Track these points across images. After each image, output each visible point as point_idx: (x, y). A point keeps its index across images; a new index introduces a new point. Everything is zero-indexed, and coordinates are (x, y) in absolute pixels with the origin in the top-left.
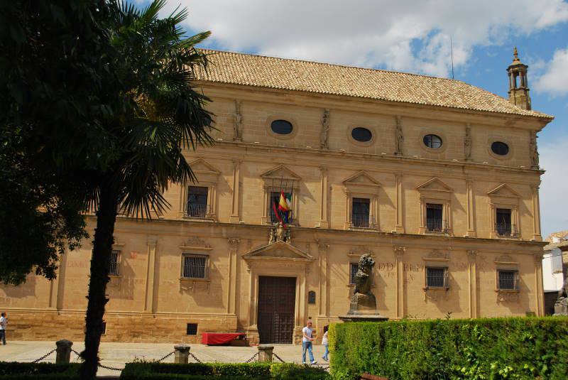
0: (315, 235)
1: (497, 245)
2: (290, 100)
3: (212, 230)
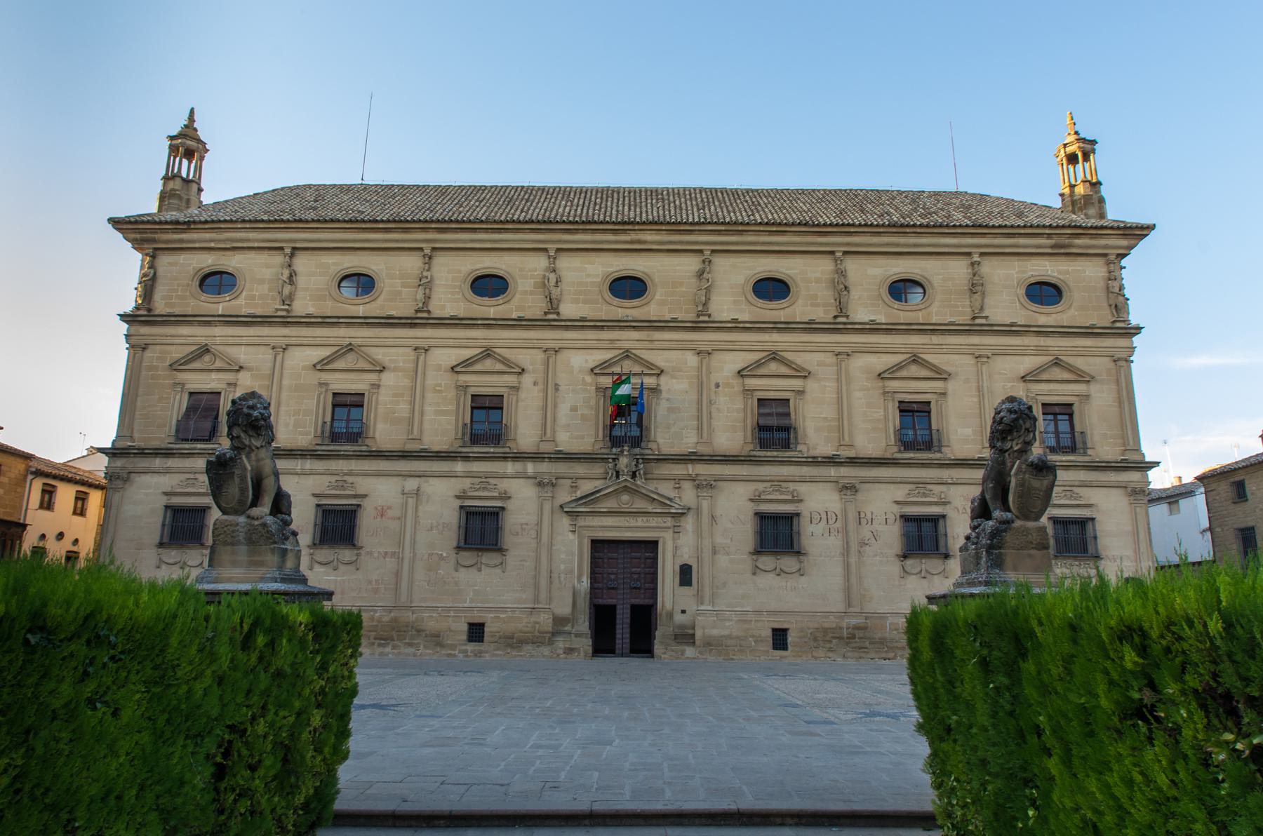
0: (690, 466)
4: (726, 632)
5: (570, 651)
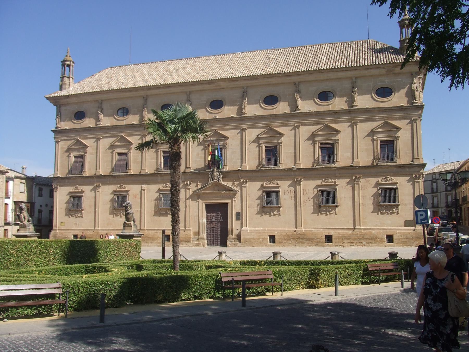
0: (239, 174)
1: (380, 170)
4: (252, 237)
5: (198, 245)
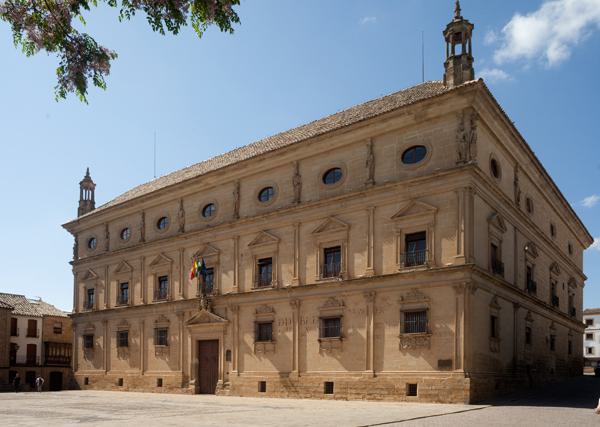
2: (207, 184)
3: (169, 308)
